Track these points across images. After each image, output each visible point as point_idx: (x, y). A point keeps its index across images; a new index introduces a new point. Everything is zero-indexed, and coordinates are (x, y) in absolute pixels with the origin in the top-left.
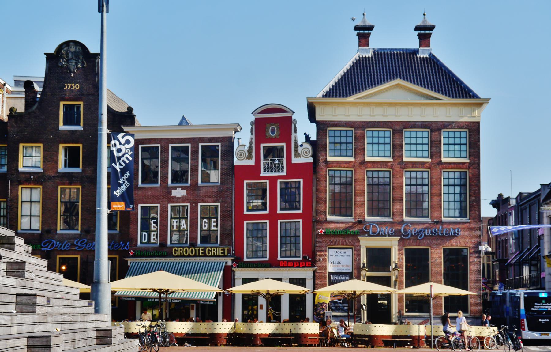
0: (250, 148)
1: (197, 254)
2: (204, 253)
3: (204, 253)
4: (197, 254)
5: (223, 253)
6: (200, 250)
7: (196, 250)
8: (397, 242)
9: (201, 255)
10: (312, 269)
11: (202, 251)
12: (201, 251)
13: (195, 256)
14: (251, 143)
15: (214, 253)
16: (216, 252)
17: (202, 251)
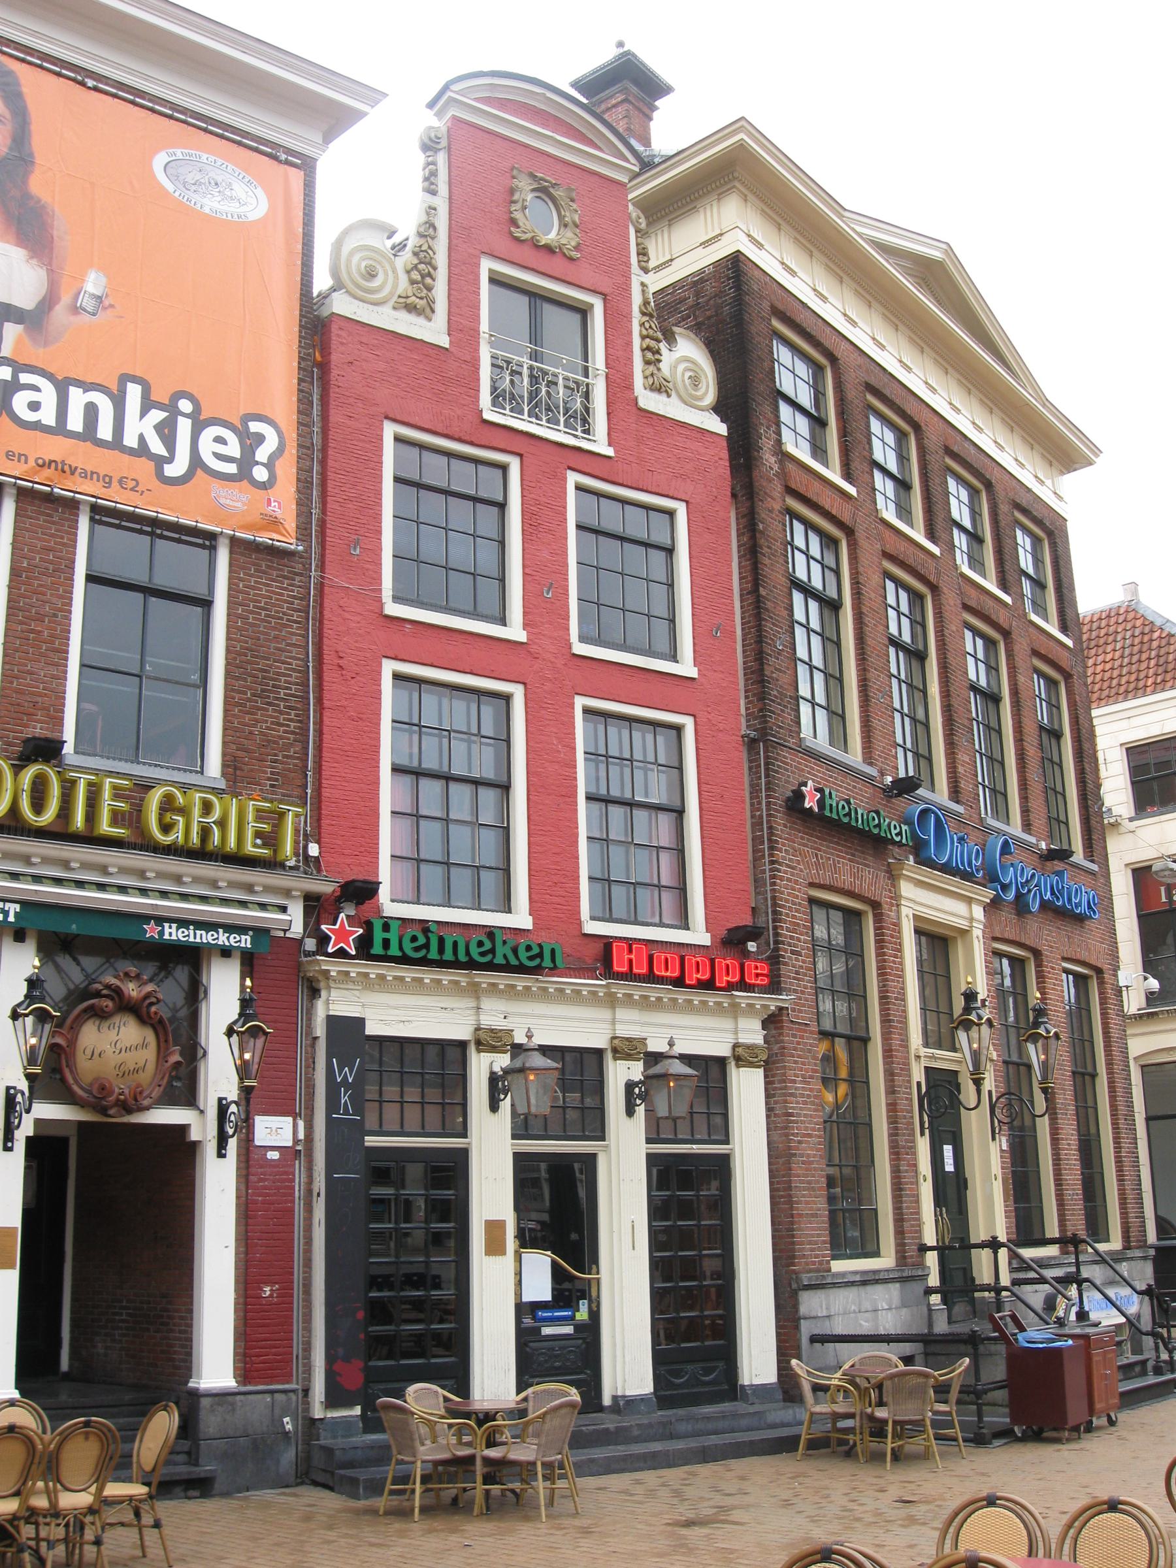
0: (424, 257)
1: (79, 820)
2: (133, 817)
3: (133, 817)
4: (79, 820)
5: (270, 839)
6: (107, 793)
7: (68, 788)
8: (978, 912)
9: (105, 827)
10: (773, 1003)
11: (122, 805)
12: (107, 802)
13: (59, 833)
14: (427, 230)
15: (205, 832)
16: (222, 823)
17: (122, 805)
